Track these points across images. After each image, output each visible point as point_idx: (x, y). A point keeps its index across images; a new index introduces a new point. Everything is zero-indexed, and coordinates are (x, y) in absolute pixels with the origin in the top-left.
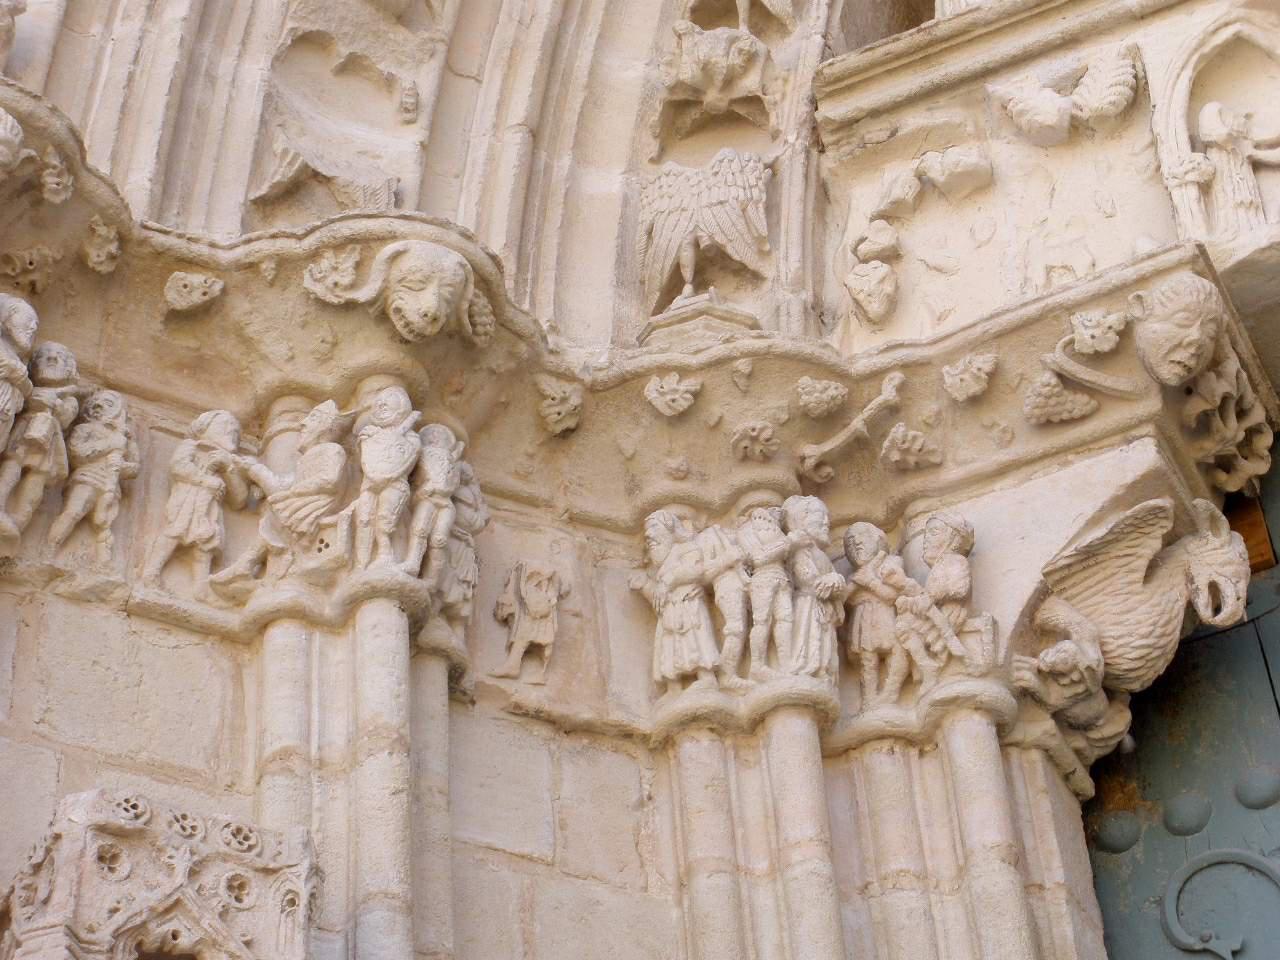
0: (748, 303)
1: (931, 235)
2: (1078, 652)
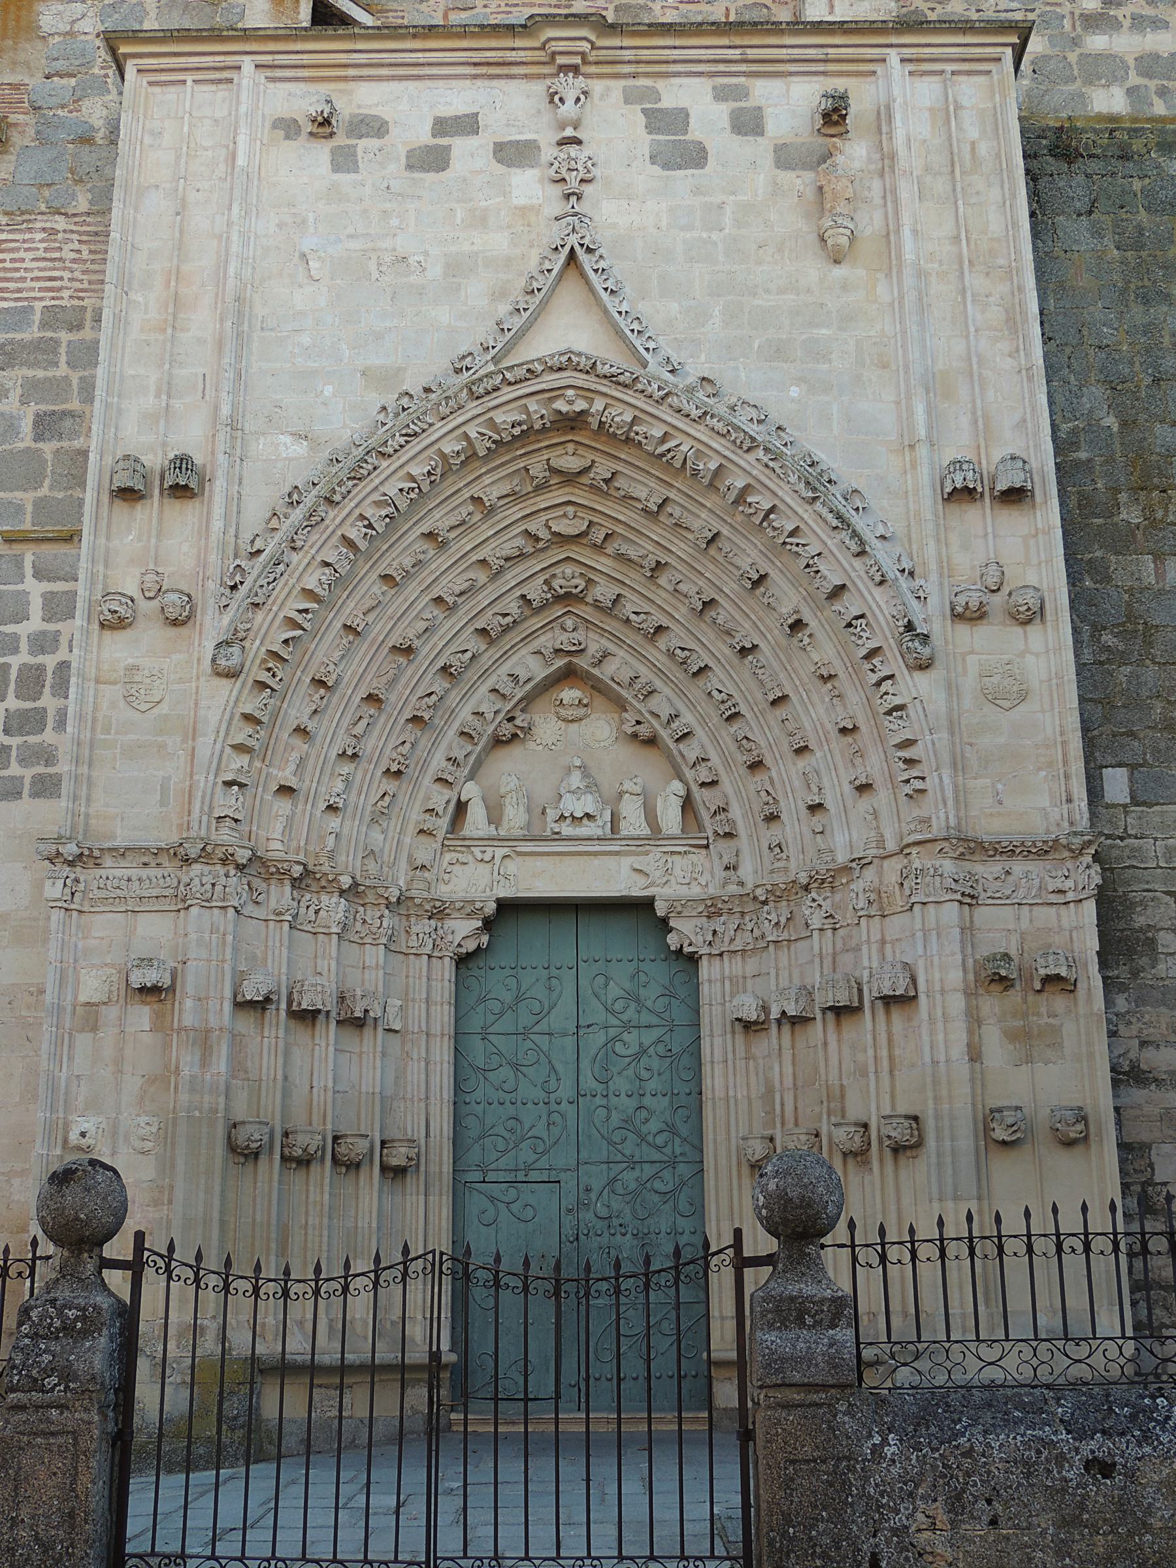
0: (427, 874)
1: (457, 868)
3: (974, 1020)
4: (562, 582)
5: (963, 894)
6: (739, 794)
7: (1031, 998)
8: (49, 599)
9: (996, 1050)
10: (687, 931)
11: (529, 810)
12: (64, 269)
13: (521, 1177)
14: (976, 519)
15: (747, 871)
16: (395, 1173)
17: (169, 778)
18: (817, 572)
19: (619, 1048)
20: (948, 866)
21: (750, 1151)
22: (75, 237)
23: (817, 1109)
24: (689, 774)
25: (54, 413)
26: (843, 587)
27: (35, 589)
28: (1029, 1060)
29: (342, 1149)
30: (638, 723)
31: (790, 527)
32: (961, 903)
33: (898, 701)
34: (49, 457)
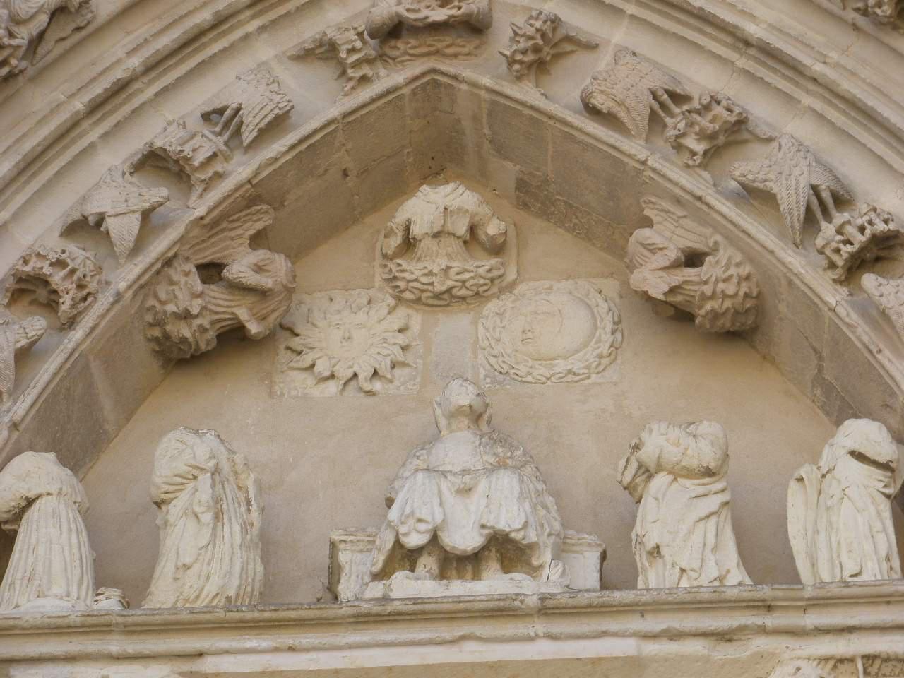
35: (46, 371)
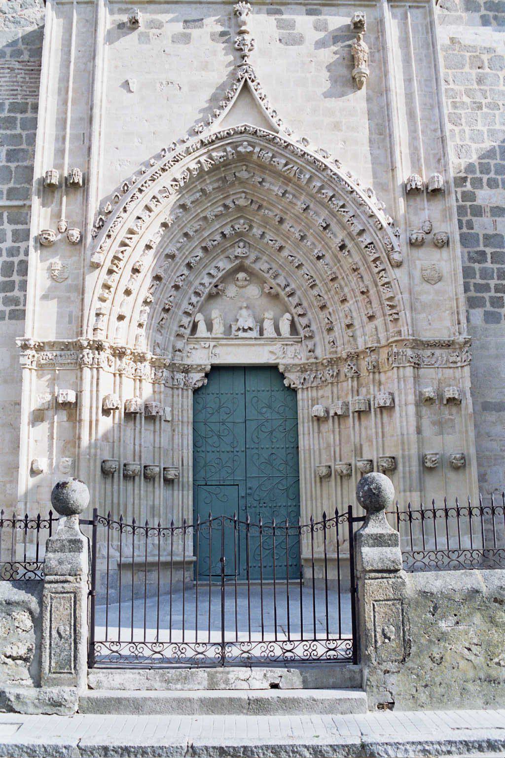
1: (194, 351)
2: (196, 386)
3: (419, 416)
4: (238, 226)
5: (415, 363)
6: (317, 320)
7: (442, 407)
8: (15, 233)
9: (428, 430)
10: (292, 379)
11: (224, 326)
12: (18, 86)
13: (222, 483)
14: (422, 202)
15: (319, 352)
16: (169, 482)
17: (72, 312)
18: (352, 224)
19: (263, 429)
20: (409, 352)
21: (321, 472)
22: (23, 71)
23: (350, 454)
24: (294, 311)
25: (15, 150)
26: (364, 230)
27: (9, 228)
28: (441, 433)
29: (148, 471)
30: (271, 288)
31: (341, 204)
32: (414, 367)
33: (387, 280)
34: (13, 169)
35: (200, 304)
